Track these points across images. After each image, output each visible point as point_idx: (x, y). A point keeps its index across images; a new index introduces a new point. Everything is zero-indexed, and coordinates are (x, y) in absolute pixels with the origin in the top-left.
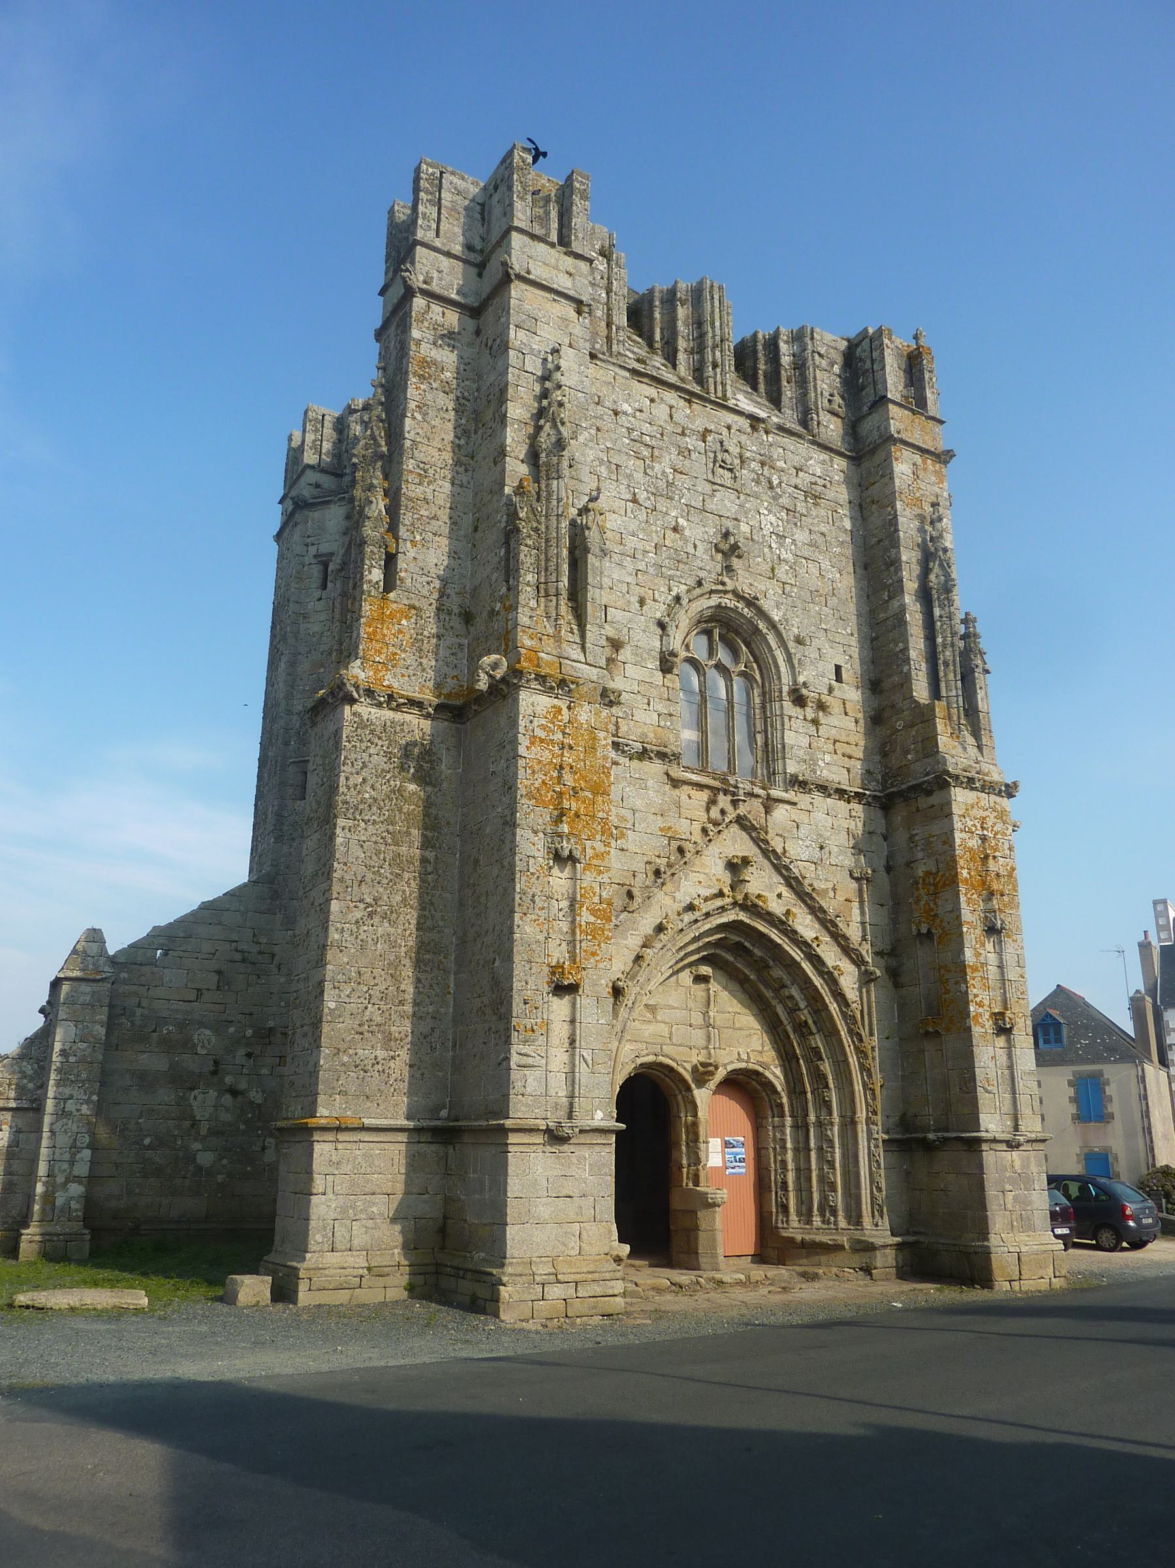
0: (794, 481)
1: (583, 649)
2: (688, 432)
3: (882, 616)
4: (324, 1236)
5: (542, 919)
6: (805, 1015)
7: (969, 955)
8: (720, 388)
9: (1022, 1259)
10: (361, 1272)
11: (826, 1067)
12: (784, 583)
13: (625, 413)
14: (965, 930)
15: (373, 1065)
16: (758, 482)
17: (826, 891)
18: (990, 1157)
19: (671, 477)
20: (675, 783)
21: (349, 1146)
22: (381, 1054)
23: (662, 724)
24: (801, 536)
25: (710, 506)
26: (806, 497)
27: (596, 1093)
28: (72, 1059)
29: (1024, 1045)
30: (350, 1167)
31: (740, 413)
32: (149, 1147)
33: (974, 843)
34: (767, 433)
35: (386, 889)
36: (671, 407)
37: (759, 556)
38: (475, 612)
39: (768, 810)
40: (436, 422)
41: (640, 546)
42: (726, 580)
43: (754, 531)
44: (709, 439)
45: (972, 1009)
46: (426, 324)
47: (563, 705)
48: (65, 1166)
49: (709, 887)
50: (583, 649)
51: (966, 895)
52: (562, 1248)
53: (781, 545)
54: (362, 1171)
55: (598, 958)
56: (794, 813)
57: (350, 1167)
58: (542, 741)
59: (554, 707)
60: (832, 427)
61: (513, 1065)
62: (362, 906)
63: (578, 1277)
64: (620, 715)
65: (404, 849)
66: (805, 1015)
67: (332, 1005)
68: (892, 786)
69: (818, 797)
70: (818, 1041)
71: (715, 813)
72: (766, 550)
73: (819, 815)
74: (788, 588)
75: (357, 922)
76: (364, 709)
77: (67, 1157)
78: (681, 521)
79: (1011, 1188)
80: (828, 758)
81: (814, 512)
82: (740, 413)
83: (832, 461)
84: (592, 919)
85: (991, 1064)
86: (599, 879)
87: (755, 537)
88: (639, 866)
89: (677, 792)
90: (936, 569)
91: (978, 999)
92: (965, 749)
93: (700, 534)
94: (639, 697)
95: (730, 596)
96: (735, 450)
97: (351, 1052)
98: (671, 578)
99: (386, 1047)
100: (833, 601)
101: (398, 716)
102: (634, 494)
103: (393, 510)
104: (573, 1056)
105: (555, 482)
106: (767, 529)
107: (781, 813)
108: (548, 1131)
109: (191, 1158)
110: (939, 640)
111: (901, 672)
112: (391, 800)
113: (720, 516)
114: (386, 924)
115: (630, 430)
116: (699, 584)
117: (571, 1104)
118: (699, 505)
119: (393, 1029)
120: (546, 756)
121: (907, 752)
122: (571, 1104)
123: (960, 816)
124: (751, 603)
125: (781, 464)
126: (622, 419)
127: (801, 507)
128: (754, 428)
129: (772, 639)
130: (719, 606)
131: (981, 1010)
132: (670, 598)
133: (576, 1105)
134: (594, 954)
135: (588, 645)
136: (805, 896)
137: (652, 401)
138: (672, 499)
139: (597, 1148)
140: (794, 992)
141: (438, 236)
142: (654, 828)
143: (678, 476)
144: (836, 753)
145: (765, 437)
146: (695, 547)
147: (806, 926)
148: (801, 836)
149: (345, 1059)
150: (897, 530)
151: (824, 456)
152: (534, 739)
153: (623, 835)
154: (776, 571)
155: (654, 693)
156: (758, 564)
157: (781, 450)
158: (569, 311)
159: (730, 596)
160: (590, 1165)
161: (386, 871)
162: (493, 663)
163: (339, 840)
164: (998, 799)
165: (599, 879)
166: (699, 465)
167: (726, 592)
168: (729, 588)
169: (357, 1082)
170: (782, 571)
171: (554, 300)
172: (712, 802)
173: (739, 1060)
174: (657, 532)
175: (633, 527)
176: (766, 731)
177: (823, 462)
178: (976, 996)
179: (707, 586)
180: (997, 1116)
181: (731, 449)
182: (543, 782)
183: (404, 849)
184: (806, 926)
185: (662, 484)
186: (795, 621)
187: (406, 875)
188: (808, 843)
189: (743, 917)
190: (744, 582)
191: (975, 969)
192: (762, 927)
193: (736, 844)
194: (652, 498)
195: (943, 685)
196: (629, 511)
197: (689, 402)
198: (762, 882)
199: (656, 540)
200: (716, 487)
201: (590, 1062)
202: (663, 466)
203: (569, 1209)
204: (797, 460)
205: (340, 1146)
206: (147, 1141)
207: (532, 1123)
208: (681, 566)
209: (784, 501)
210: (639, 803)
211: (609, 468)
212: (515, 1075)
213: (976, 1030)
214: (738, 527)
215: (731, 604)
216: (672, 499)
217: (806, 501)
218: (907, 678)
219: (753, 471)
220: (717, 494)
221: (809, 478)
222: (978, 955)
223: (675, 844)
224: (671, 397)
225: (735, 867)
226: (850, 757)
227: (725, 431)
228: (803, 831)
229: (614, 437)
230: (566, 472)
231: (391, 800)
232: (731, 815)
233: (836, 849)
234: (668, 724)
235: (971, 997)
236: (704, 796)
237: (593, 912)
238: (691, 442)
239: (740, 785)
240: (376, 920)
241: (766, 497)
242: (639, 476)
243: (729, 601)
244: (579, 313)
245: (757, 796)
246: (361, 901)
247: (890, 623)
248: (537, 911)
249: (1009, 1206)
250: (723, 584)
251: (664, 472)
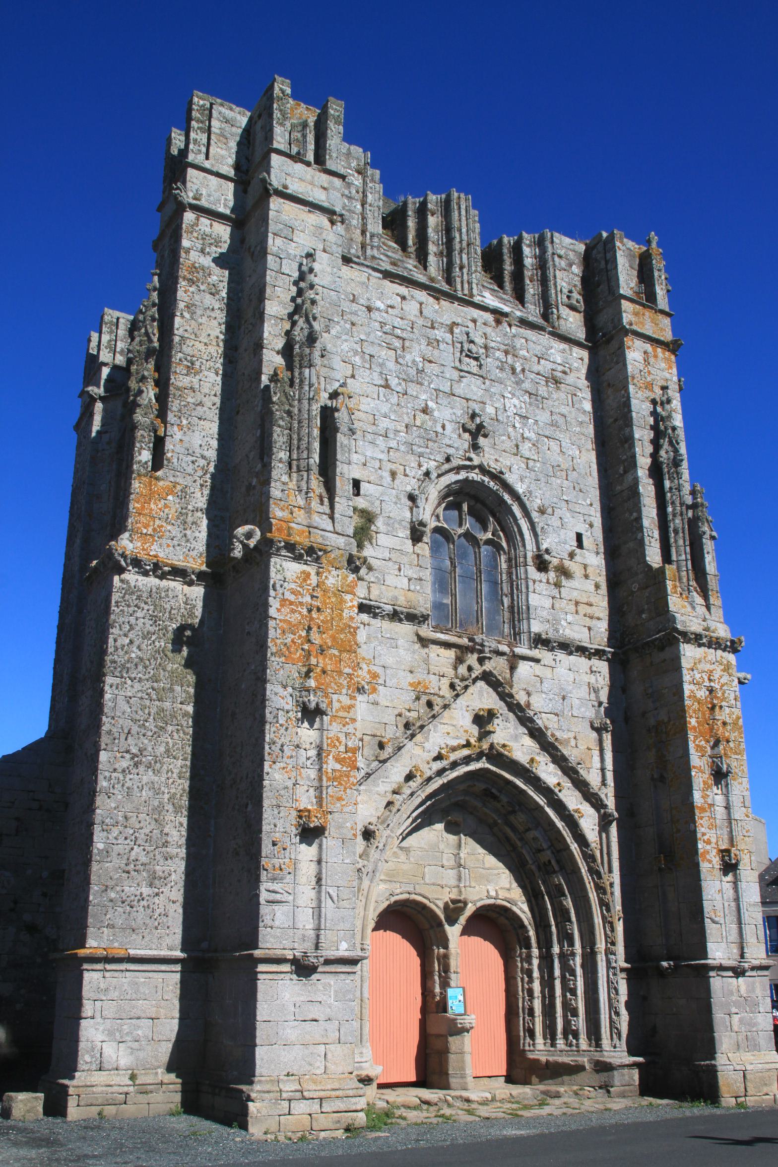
0: (536, 368)
1: (332, 517)
2: (436, 325)
3: (619, 488)
4: (92, 1057)
5: (290, 767)
7: (697, 796)
8: (466, 286)
9: (748, 1076)
10: (126, 1089)
11: (569, 903)
12: (528, 459)
13: (378, 309)
14: (693, 774)
15: (139, 901)
17: (568, 741)
18: (717, 983)
19: (421, 365)
20: (424, 642)
21: (116, 974)
22: (146, 891)
23: (412, 588)
24: (544, 417)
25: (457, 391)
26: (547, 382)
27: (341, 926)
29: (749, 879)
30: (117, 994)
33: (702, 694)
34: (510, 326)
35: (150, 741)
36: (421, 304)
37: (504, 435)
38: (237, 490)
39: (513, 668)
41: (392, 426)
42: (473, 455)
43: (499, 413)
44: (457, 330)
45: (700, 846)
46: (195, 234)
47: (312, 569)
49: (457, 738)
50: (332, 517)
51: (694, 742)
52: (308, 1068)
53: (525, 425)
54: (128, 997)
55: (344, 803)
56: (537, 669)
57: (117, 994)
58: (291, 603)
59: (303, 572)
60: (571, 320)
61: (262, 900)
62: (128, 756)
63: (322, 1094)
64: (372, 580)
65: (167, 705)
67: (101, 846)
69: (561, 655)
71: (462, 670)
72: (510, 429)
74: (531, 463)
75: (124, 771)
78: (430, 404)
79: (736, 1011)
81: (555, 396)
83: (571, 350)
84: (338, 766)
85: (718, 897)
86: (345, 729)
87: (500, 418)
88: (390, 718)
89: (426, 650)
90: (666, 446)
91: (706, 838)
92: (694, 608)
93: (448, 414)
94: (390, 564)
96: (480, 341)
97: (118, 888)
100: (573, 475)
101: (165, 583)
102: (387, 380)
103: (163, 398)
104: (319, 892)
105: (307, 370)
106: (511, 411)
107: (524, 668)
108: (295, 962)
110: (670, 509)
111: (636, 539)
112: (156, 659)
113: (467, 400)
114: (150, 773)
115: (382, 324)
116: (448, 460)
117: (318, 936)
118: (447, 390)
119: (157, 868)
120: (295, 618)
121: (642, 612)
122: (318, 936)
123: (688, 669)
124: (497, 477)
125: (523, 353)
126: (375, 315)
127: (543, 391)
128: (498, 322)
129: (516, 509)
131: (708, 847)
132: (420, 472)
133: (322, 937)
134: (340, 799)
135: (336, 516)
136: (548, 746)
137: (404, 298)
138: (421, 384)
139: (343, 976)
141: (207, 158)
142: (405, 684)
143: (427, 364)
144: (577, 612)
145: (508, 329)
146: (443, 427)
147: (549, 774)
148: (545, 690)
149: (113, 895)
150: (630, 411)
151: (564, 346)
152: (284, 602)
153: (374, 690)
154: (520, 448)
155: (405, 560)
156: (503, 442)
157: (523, 341)
158: (324, 220)
160: (335, 991)
161: (150, 724)
162: (246, 534)
164: (725, 654)
165: (345, 729)
166: (447, 355)
167: (472, 468)
168: (476, 462)
169: (124, 916)
170: (526, 449)
171: (310, 211)
172: (459, 660)
173: (489, 897)
174: (408, 414)
175: (385, 408)
176: (512, 594)
177: (563, 351)
178: (704, 834)
179: (455, 462)
180: (724, 945)
181: (477, 340)
182: (293, 641)
183: (167, 705)
184: (549, 774)
185: (413, 372)
186: (538, 493)
187: (170, 728)
188: (551, 696)
190: (489, 457)
191: (703, 810)
193: (482, 697)
194: (403, 383)
195: (673, 550)
196: (381, 395)
197: (438, 299)
199: (406, 420)
200: (462, 374)
201: (335, 899)
202: (414, 355)
203: (315, 1031)
204: (538, 350)
205: (107, 974)
207: (279, 953)
208: (430, 444)
209: (527, 385)
210: (390, 661)
211: (362, 358)
212: (264, 910)
213: (704, 866)
214: (483, 410)
216: (421, 384)
217: (547, 386)
218: (641, 544)
219: (497, 359)
220: (464, 380)
221: (550, 366)
222: (705, 797)
223: (424, 699)
225: (483, 720)
226: (591, 618)
227: (471, 325)
228: (546, 686)
229: (367, 330)
230: (317, 360)
231: (156, 659)
232: (478, 670)
233: (577, 702)
234: (418, 588)
235: (699, 835)
236: (451, 654)
237: (338, 760)
238: (439, 334)
239: (486, 644)
240: (142, 769)
241: (510, 381)
242: (391, 365)
243: (475, 476)
244: (333, 223)
245: (502, 654)
246: (128, 752)
248: (285, 759)
249: (735, 1028)
250: (470, 459)
251: (414, 361)
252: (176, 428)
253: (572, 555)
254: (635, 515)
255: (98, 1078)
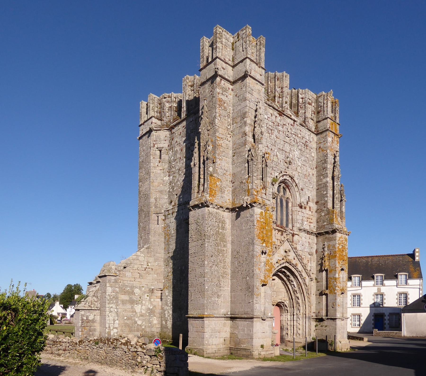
3: (320, 183)
6: (297, 289)
16: (294, 141)
22: (217, 299)
28: (111, 297)
31: (292, 119)
32: (125, 320)
40: (223, 120)
48: (113, 325)
53: (299, 160)
66: (297, 289)
67: (207, 288)
68: (319, 230)
70: (298, 295)
73: (303, 238)
76: (211, 209)
77: (113, 322)
80: (306, 223)
82: (292, 119)
95: (288, 176)
96: (290, 131)
98: (275, 170)
99: (218, 298)
101: (218, 211)
106: (296, 156)
107: (296, 237)
109: (136, 322)
116: (281, 172)
117: (264, 312)
121: (325, 222)
122: (264, 312)
130: (285, 179)
140: (295, 283)
151: (309, 133)
159: (288, 176)
161: (216, 253)
163: (206, 245)
179: (283, 173)
183: (220, 247)
187: (220, 254)
189: (287, 265)
192: (290, 267)
193: (287, 246)
198: (291, 256)
206: (125, 318)
215: (288, 179)
224: (276, 113)
227: (287, 125)
238: (280, 128)
241: (296, 145)
242: (268, 139)
247: (322, 185)
250: (286, 172)
252: (218, 160)
253: (307, 203)
254: (325, 192)
255: (209, 347)
